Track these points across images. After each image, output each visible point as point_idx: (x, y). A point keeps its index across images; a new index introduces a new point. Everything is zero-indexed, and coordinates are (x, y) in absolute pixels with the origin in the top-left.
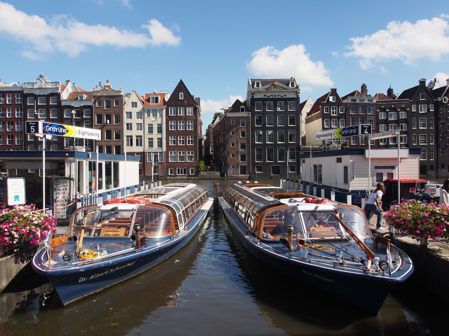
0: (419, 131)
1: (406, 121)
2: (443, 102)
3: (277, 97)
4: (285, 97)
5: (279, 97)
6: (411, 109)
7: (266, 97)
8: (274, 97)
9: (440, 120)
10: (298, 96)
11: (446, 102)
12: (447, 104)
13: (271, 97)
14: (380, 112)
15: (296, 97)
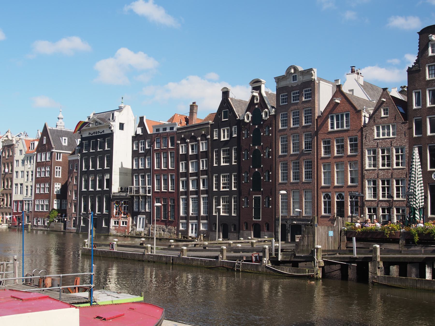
0: (220, 170)
1: (205, 154)
2: (246, 120)
3: (98, 134)
4: (103, 133)
5: (100, 134)
6: (212, 136)
7: (90, 135)
8: (95, 135)
9: (242, 151)
10: (112, 131)
11: (248, 121)
12: (250, 122)
13: (93, 135)
14: (181, 144)
15: (110, 132)
